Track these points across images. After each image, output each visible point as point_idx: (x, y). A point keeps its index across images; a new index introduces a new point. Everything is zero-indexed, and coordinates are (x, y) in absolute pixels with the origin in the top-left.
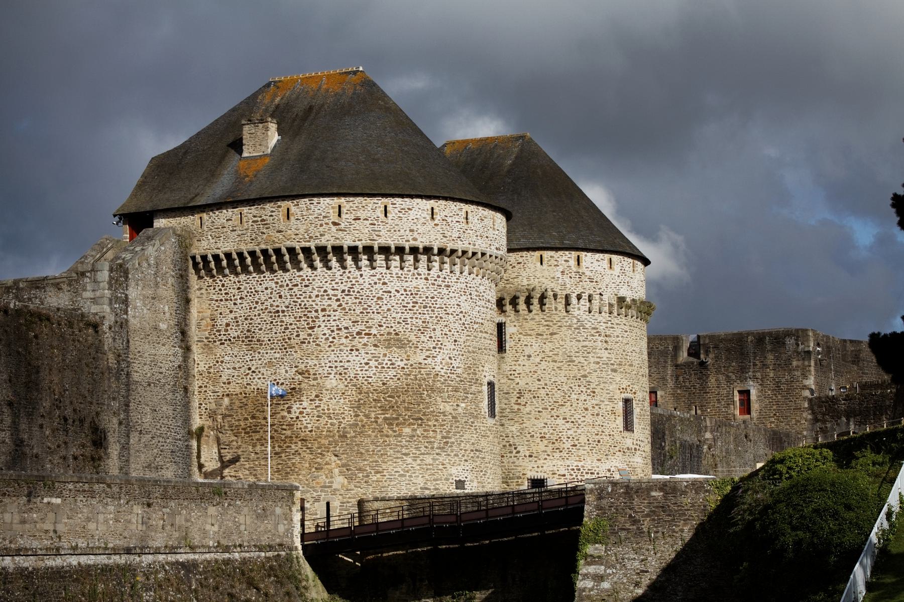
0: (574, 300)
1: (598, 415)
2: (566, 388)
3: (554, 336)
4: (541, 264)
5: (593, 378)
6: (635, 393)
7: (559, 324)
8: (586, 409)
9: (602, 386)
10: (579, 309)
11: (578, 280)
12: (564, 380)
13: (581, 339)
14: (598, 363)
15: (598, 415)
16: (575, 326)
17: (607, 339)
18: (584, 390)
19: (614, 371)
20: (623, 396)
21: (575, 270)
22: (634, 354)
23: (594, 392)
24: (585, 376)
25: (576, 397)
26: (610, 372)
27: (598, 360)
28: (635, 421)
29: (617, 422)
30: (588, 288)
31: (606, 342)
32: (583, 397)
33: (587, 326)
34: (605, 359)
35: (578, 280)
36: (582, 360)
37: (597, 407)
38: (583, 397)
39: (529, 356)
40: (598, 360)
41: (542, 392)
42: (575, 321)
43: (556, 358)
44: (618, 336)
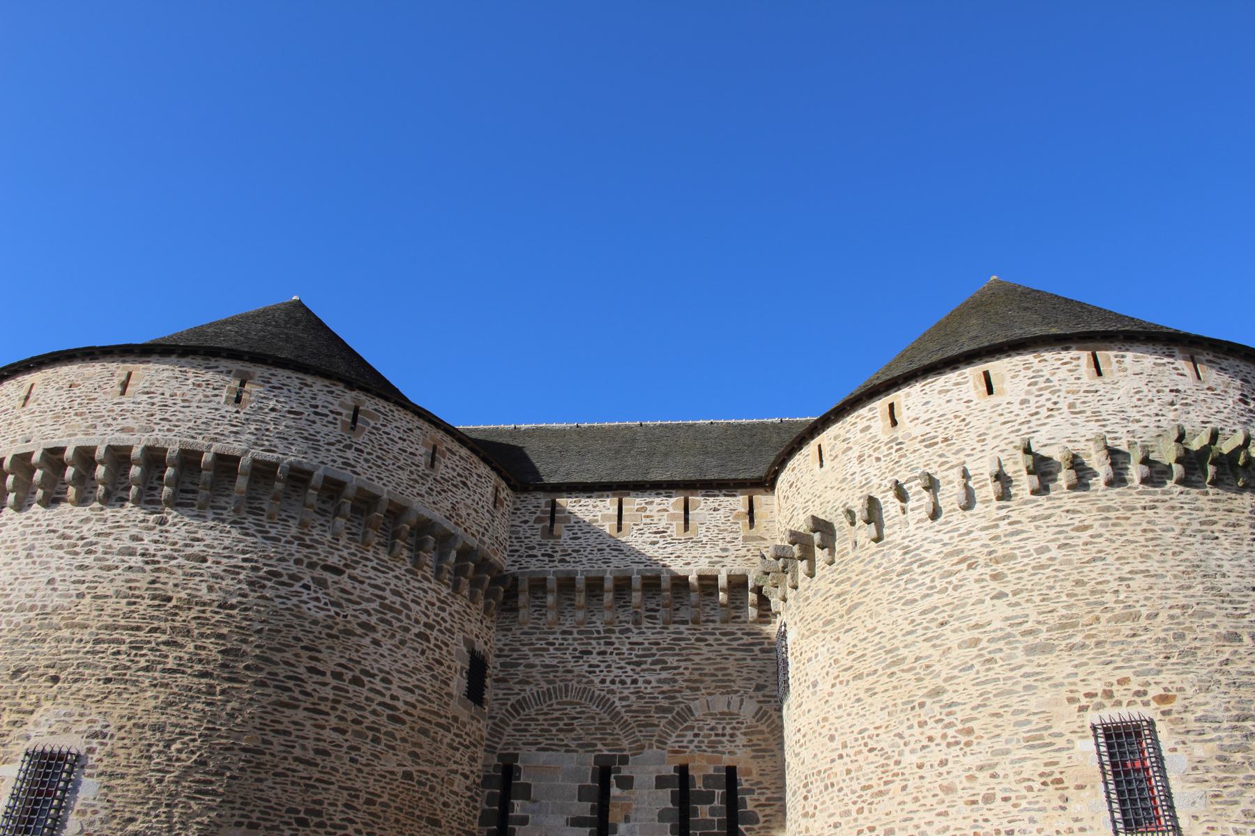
0: (890, 506)
1: (988, 799)
2: (885, 741)
3: (855, 613)
4: (821, 466)
5: (964, 691)
6: (1164, 699)
7: (863, 578)
8: (948, 790)
9: (995, 705)
10: (905, 524)
11: (895, 456)
12: (881, 718)
13: (917, 594)
14: (976, 642)
15: (988, 799)
16: (899, 568)
17: (1000, 568)
18: (937, 732)
19: (1046, 648)
20: (1092, 717)
21: (885, 438)
22: (1139, 582)
23: (970, 731)
24: (937, 692)
25: (915, 759)
26: (1020, 657)
27: (976, 634)
28: (1176, 787)
29: (1074, 808)
30: (923, 460)
31: (995, 577)
32: (934, 755)
33: (929, 556)
34: (997, 624)
35: (895, 456)
36: (925, 649)
37: (983, 776)
38: (934, 755)
39: (815, 684)
40: (976, 634)
41: (839, 767)
42: (898, 553)
43: (859, 667)
44: (1041, 550)
